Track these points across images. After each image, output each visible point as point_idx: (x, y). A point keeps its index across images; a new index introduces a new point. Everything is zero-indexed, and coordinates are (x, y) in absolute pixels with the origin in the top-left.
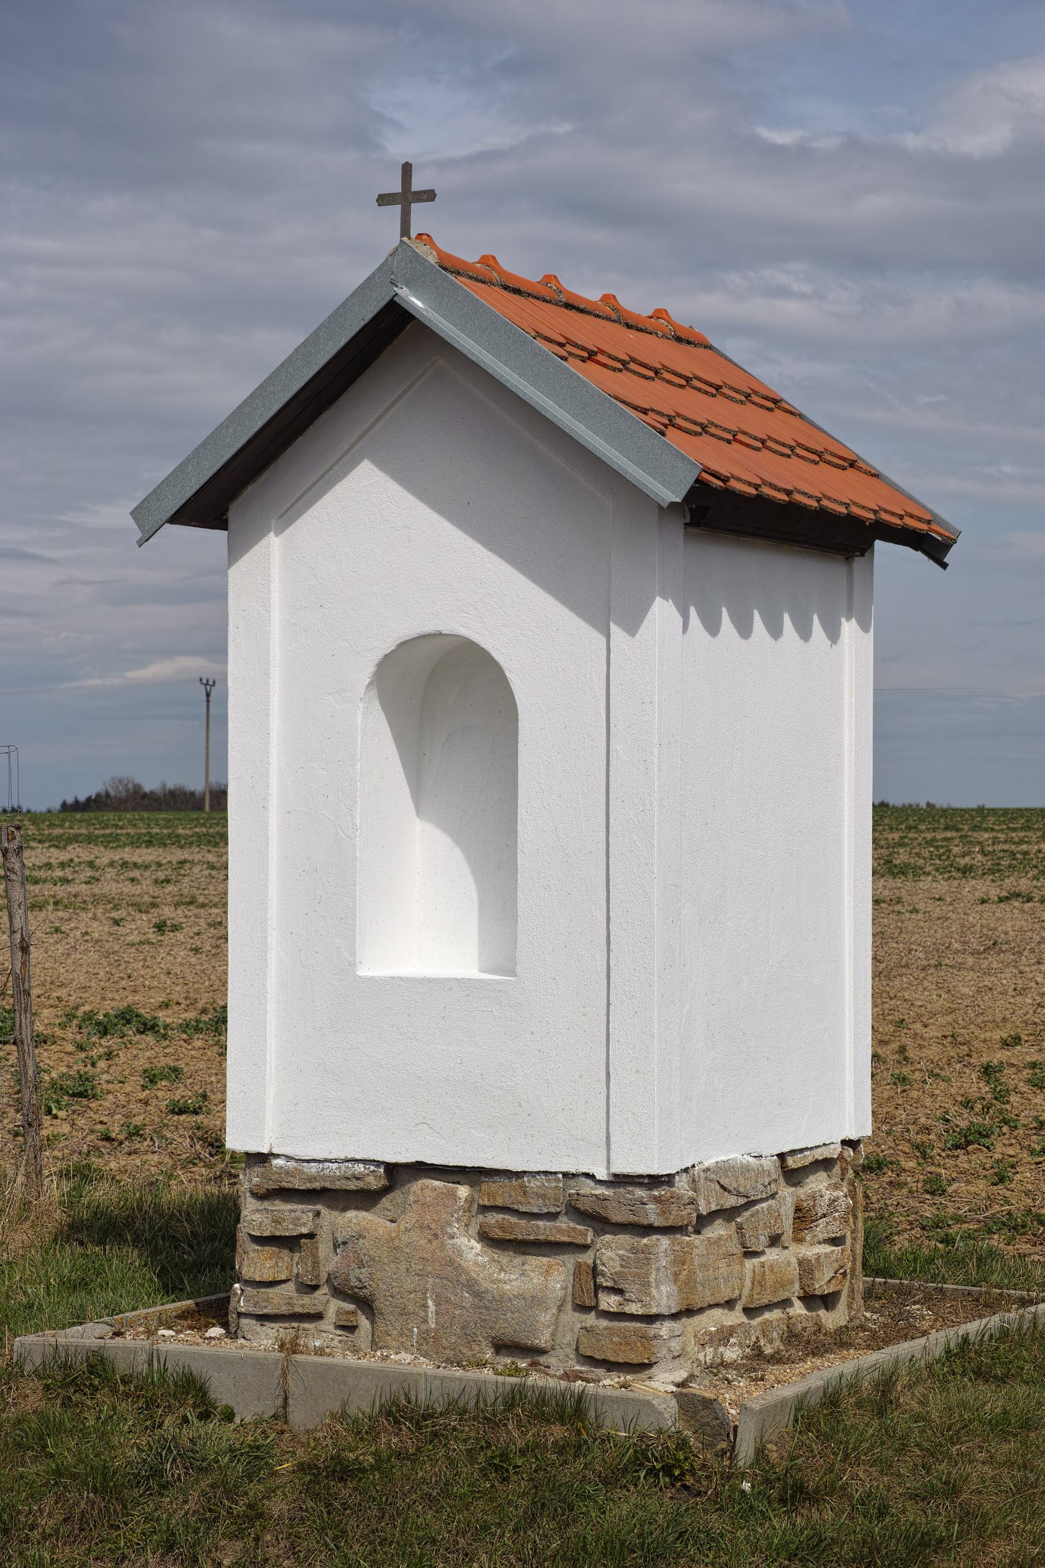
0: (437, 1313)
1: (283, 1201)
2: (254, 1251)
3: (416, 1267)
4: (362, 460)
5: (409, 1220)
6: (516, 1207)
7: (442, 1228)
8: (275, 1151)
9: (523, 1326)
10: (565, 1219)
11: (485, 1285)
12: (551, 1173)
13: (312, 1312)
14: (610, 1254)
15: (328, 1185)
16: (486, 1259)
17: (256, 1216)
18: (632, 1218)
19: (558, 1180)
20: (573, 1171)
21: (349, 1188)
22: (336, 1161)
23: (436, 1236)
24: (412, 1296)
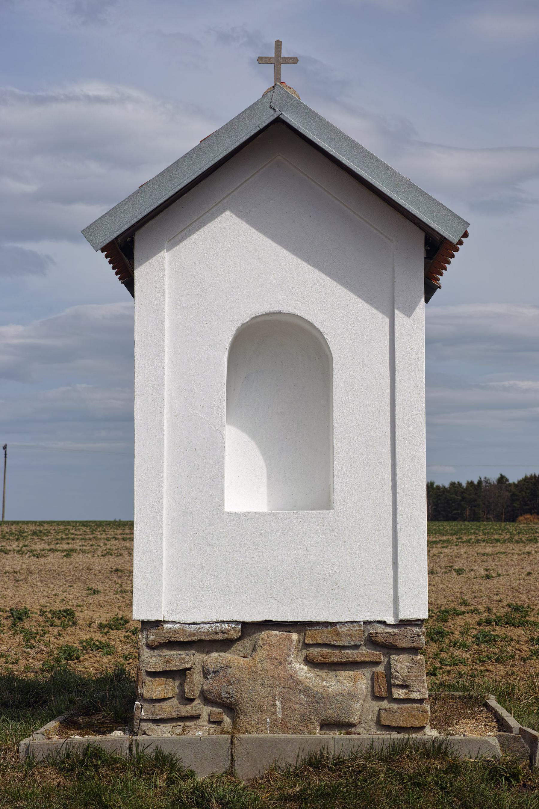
0: (283, 709)
1: (167, 649)
2: (149, 681)
3: (267, 682)
4: (226, 210)
5: (261, 654)
6: (332, 643)
7: (284, 658)
8: (166, 619)
9: (343, 711)
10: (364, 648)
11: (316, 689)
12: (355, 622)
13: (194, 714)
14: (400, 665)
15: (203, 638)
16: (312, 675)
17: (153, 660)
18: (412, 645)
19: (361, 626)
20: (372, 620)
21: (218, 639)
22: (209, 623)
23: (280, 663)
24: (266, 699)
